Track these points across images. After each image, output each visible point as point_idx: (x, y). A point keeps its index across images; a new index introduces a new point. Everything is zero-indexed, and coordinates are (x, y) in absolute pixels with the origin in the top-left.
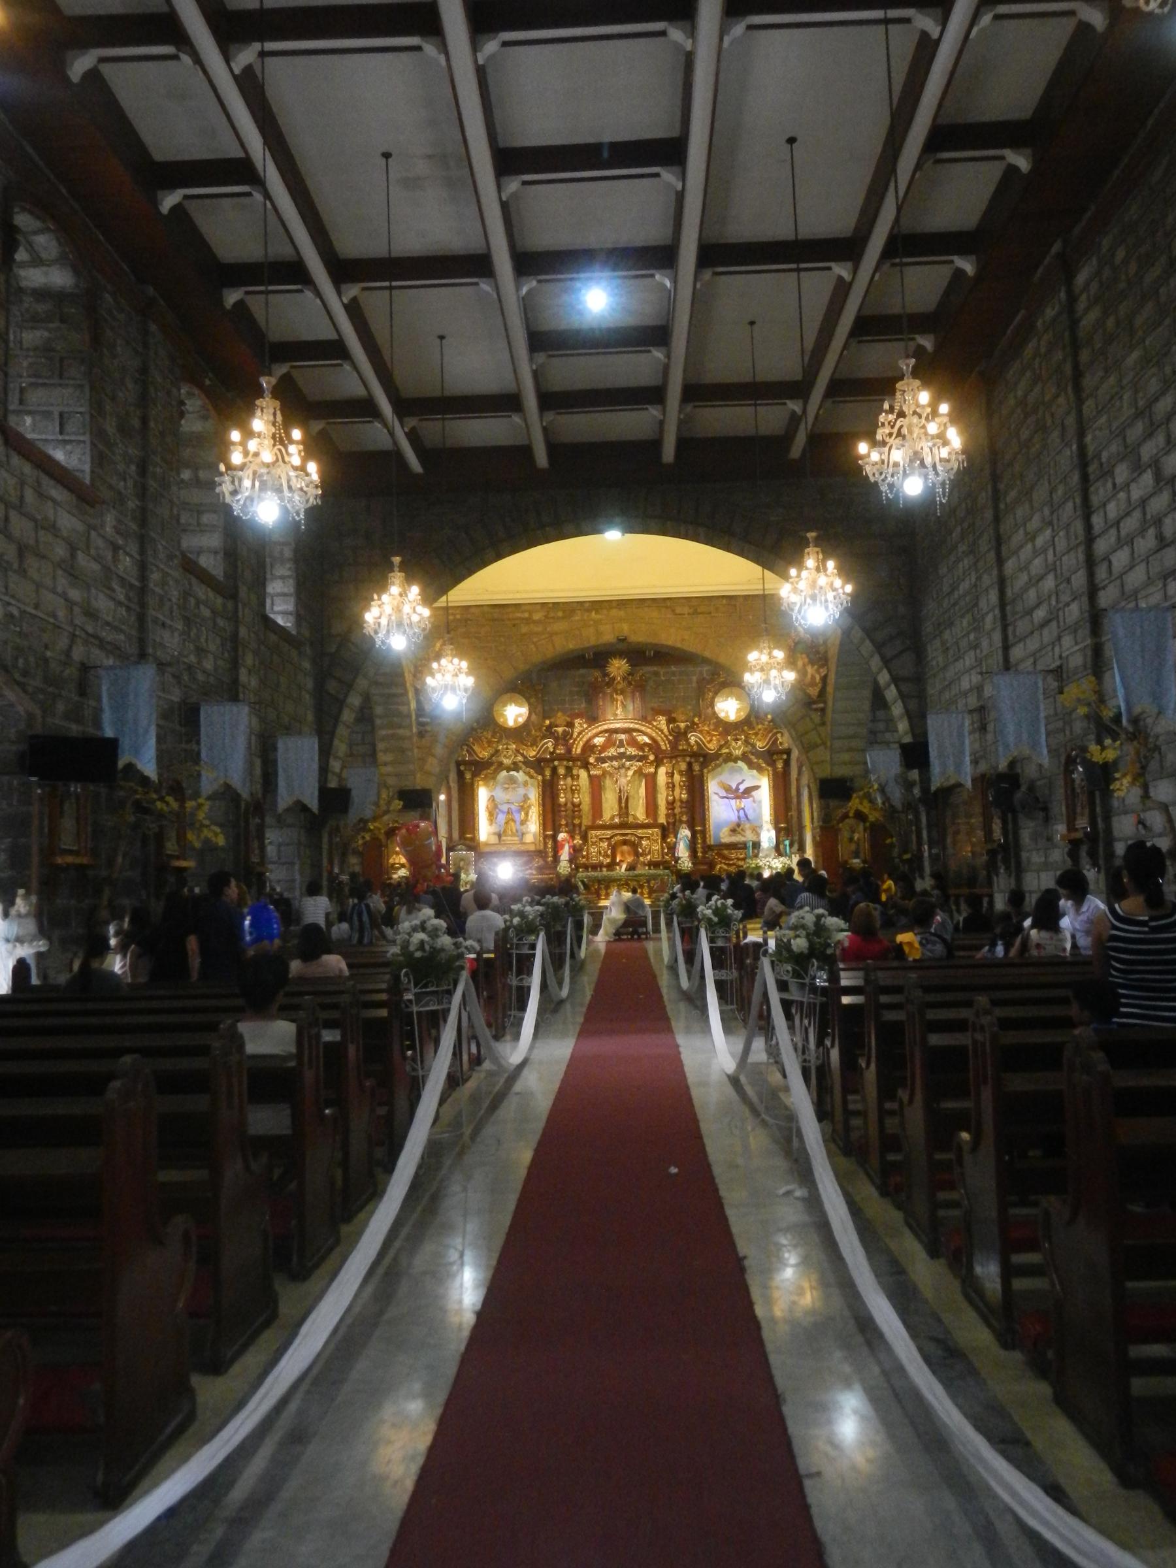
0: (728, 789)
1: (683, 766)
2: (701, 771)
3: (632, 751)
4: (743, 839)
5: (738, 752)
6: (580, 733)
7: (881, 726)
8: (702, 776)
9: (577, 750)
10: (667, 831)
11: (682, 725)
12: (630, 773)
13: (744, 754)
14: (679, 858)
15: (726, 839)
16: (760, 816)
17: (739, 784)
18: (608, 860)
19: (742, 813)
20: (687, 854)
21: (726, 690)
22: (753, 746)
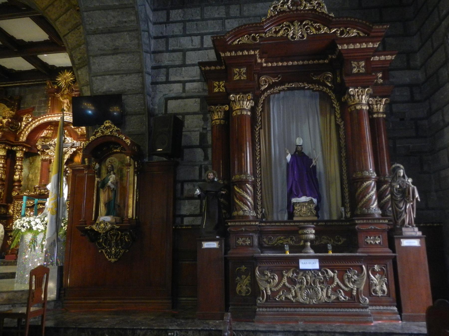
7: (177, 29)
9: (23, 138)
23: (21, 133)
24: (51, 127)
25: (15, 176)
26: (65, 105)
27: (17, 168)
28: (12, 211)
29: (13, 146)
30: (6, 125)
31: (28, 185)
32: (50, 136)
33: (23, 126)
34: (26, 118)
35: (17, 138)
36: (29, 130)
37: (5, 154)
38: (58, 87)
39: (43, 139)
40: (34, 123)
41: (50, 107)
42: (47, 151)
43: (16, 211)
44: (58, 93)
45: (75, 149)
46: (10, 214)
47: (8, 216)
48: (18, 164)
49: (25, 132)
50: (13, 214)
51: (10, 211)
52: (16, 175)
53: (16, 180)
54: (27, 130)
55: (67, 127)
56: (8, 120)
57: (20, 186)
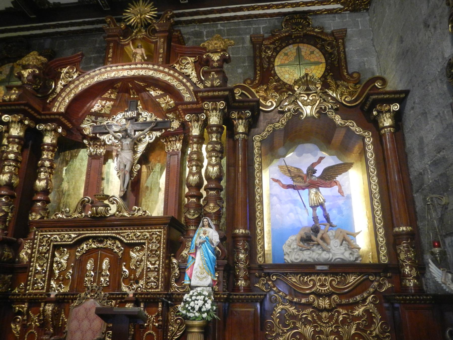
0: (294, 174)
1: (214, 120)
2: (248, 133)
3: (146, 116)
4: (325, 256)
5: (307, 110)
6: (65, 86)
8: (248, 146)
10: (176, 231)
11: (216, 57)
12: (141, 148)
13: (321, 112)
14: (192, 288)
15: (294, 254)
16: (349, 220)
17: (313, 165)
18: (65, 289)
19: (319, 209)
20: (209, 281)
21: (291, 49)
22: (333, 98)
23: (55, 100)
24: (112, 93)
25: (37, 182)
26: (139, 58)
27: (43, 166)
28: (27, 253)
29: (39, 122)
30: (29, 80)
31: (59, 203)
32: (108, 112)
33: (60, 86)
34: (67, 73)
35: (47, 107)
36: (72, 95)
37: (21, 134)
38: (127, 26)
39: (93, 118)
40: (83, 82)
41: (110, 59)
42: (102, 137)
43: (36, 255)
44: (125, 37)
45: (158, 134)
46: (21, 260)
47: (17, 265)
48: (45, 156)
49: (64, 99)
50: (30, 261)
51: (23, 254)
52: (40, 180)
53: (39, 190)
54: (68, 94)
55: (143, 94)
56: (34, 71)
57: (48, 201)
